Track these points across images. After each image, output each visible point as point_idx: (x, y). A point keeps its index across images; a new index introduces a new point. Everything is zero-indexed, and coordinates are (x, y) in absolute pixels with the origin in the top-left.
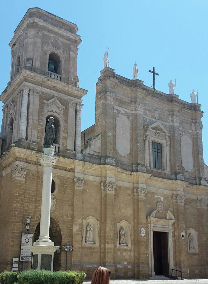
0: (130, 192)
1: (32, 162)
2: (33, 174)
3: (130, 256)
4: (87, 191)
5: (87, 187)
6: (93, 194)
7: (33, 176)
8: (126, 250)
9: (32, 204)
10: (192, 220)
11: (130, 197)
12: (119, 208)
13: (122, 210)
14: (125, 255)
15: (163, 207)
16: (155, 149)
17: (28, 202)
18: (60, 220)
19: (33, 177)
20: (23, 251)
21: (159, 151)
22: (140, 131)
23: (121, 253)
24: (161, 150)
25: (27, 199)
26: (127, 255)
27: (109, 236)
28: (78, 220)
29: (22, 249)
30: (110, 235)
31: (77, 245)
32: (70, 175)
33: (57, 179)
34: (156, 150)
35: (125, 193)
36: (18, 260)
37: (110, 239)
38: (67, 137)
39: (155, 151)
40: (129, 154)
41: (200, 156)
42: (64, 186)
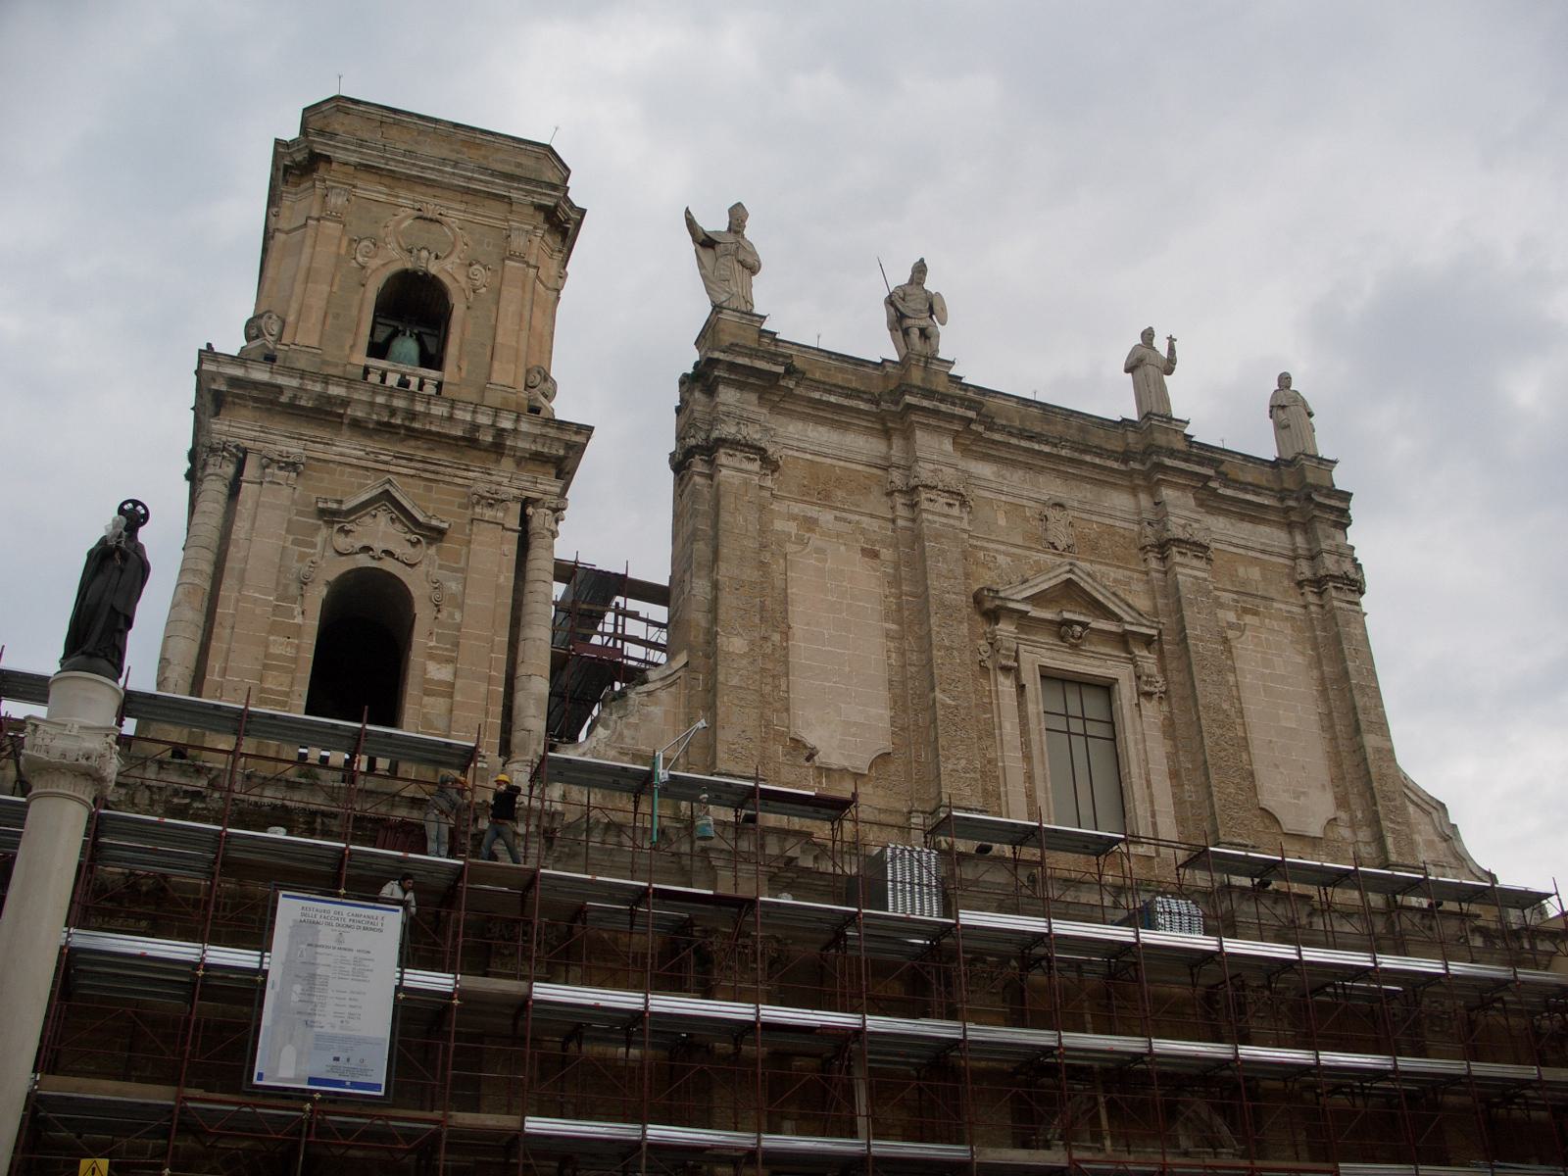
16: (1067, 716)
21: (1093, 729)
24: (1112, 723)
34: (1076, 726)
38: (452, 685)
39: (1069, 733)
41: (1370, 740)
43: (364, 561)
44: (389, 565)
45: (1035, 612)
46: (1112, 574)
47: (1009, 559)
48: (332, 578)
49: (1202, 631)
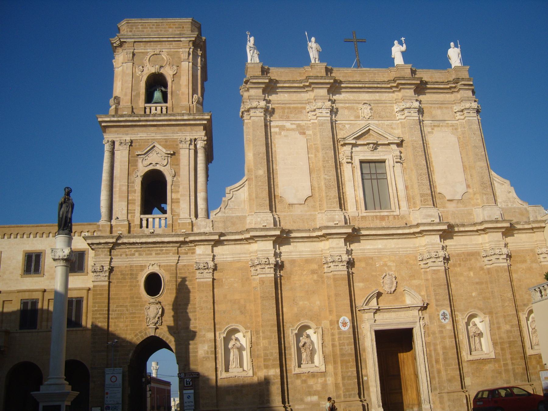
2: (121, 271)
3: (324, 385)
4: (222, 281)
5: (221, 274)
6: (236, 285)
7: (122, 274)
8: (313, 375)
9: (122, 320)
10: (474, 294)
11: (315, 277)
12: (294, 301)
13: (301, 303)
14: (312, 383)
17: (116, 318)
19: (122, 276)
23: (304, 382)
25: (114, 313)
26: (316, 383)
28: (207, 334)
29: (107, 393)
30: (272, 353)
34: (374, 177)
35: (304, 270)
37: (270, 359)
43: (151, 167)
44: (158, 167)
45: (359, 142)
46: (386, 123)
47: (349, 126)
48: (142, 174)
49: (416, 138)
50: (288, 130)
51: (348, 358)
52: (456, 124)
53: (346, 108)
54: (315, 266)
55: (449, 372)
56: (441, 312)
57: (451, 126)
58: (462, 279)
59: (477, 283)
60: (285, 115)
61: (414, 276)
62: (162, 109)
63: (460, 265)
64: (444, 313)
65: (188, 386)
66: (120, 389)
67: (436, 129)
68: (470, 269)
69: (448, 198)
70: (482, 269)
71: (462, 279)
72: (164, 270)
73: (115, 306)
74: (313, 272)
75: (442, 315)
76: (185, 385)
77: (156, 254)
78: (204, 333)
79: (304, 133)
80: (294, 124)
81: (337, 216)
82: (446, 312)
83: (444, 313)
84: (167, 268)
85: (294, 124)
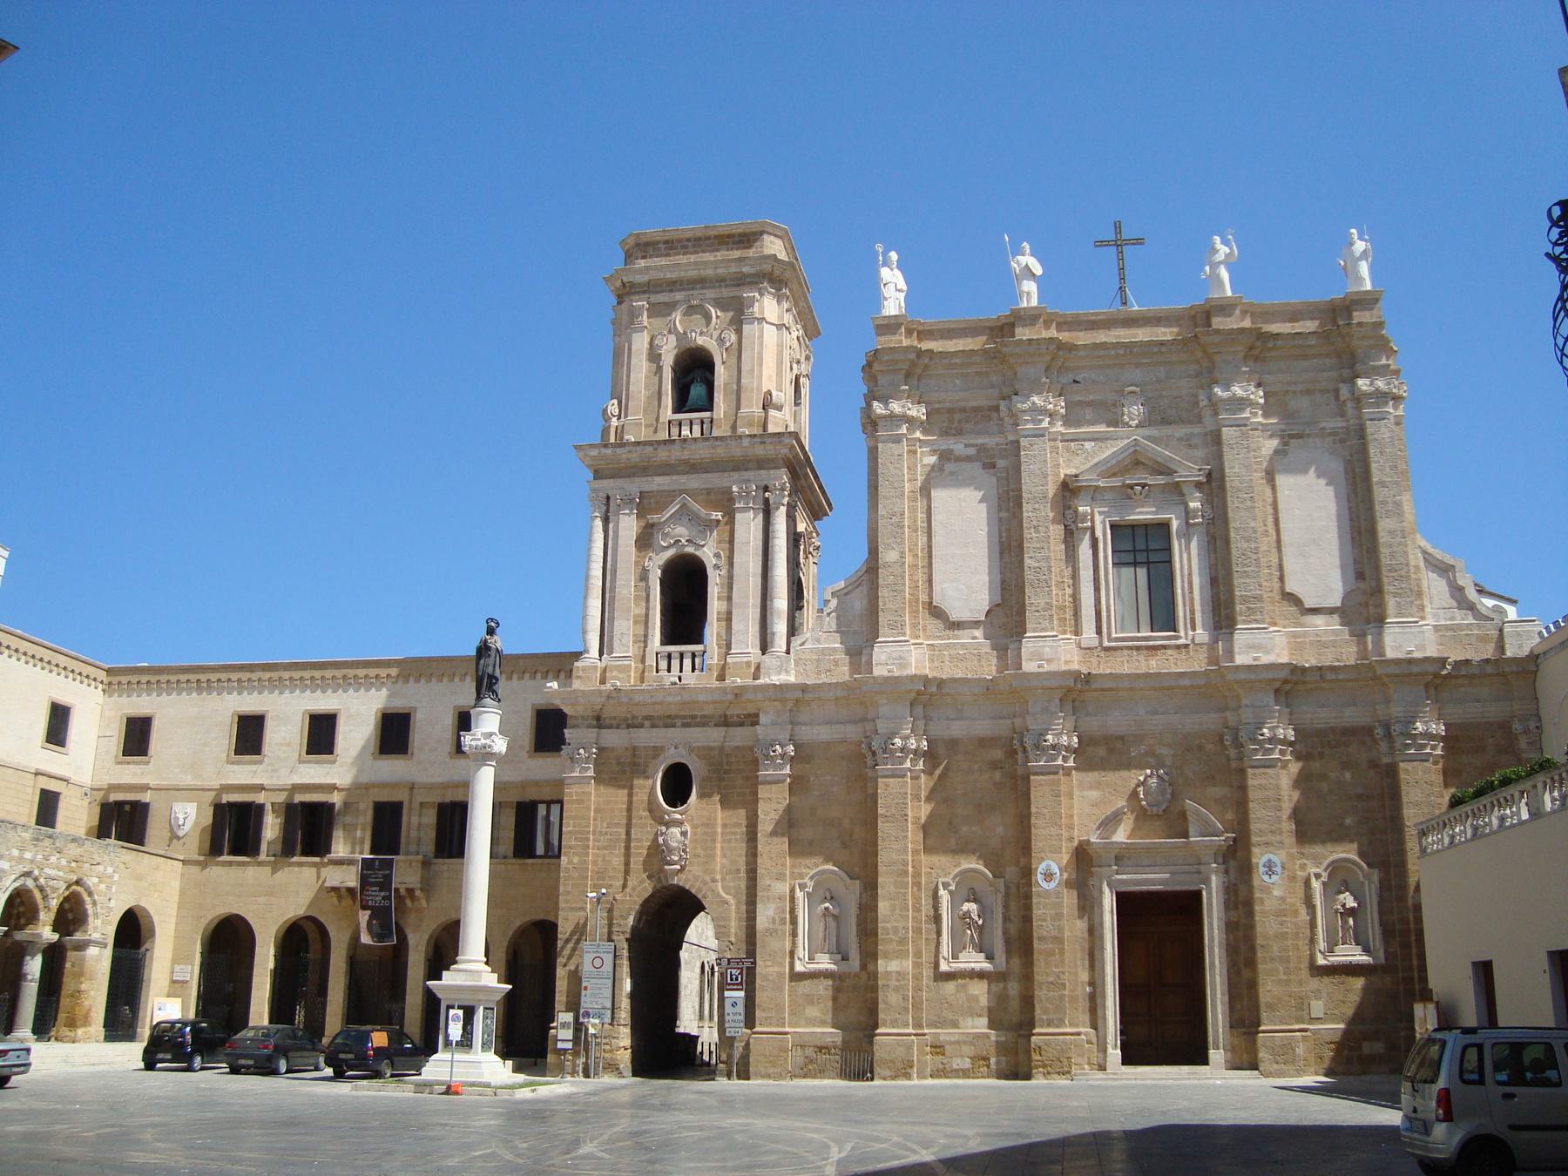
0: (997, 754)
1: (615, 722)
4: (808, 781)
6: (835, 789)
10: (1348, 821)
11: (997, 776)
14: (977, 992)
15: (1169, 791)
17: (605, 848)
18: (709, 894)
20: (588, 992)
22: (1037, 506)
27: (890, 932)
28: (773, 884)
31: (771, 969)
32: (739, 737)
33: (697, 759)
36: (571, 1019)
40: (999, 605)
42: (723, 780)
50: (958, 459)
51: (1051, 946)
52: (1343, 428)
53: (1089, 404)
54: (997, 754)
55: (1269, 988)
56: (1264, 859)
57: (1330, 434)
58: (1324, 786)
59: (1359, 797)
60: (954, 426)
61: (1213, 778)
62: (702, 423)
63: (1321, 756)
64: (1270, 860)
65: (733, 984)
66: (610, 982)
67: (1293, 442)
68: (1345, 765)
69: (1308, 604)
70: (1374, 765)
71: (1324, 786)
72: (697, 756)
73: (605, 825)
74: (994, 765)
75: (1264, 866)
76: (729, 981)
77: (686, 725)
78: (768, 882)
79: (993, 466)
80: (972, 445)
81: (1047, 649)
82: (1275, 859)
83: (1270, 860)
84: (704, 752)
85: (972, 445)
